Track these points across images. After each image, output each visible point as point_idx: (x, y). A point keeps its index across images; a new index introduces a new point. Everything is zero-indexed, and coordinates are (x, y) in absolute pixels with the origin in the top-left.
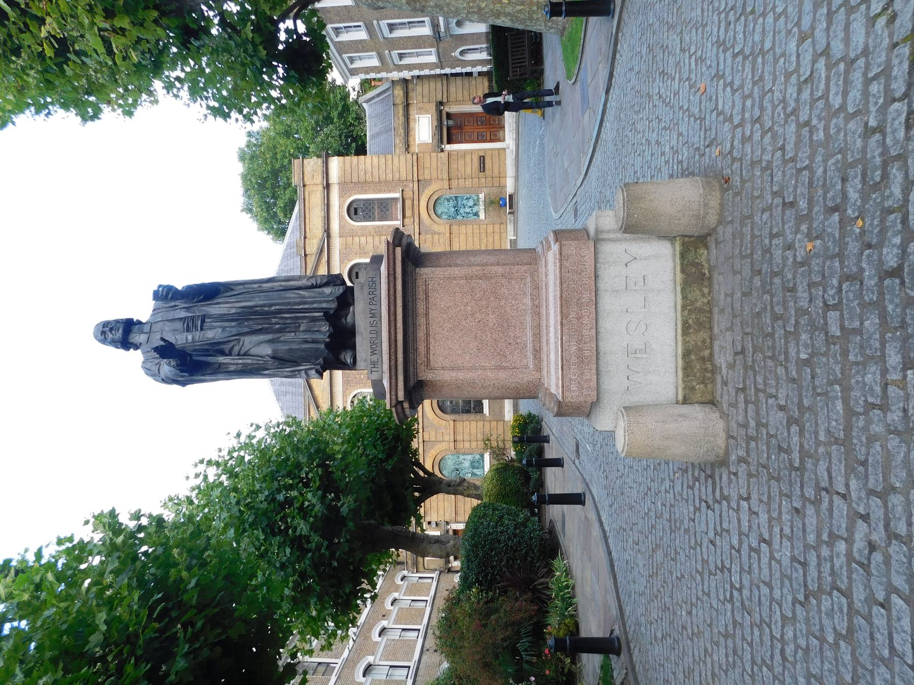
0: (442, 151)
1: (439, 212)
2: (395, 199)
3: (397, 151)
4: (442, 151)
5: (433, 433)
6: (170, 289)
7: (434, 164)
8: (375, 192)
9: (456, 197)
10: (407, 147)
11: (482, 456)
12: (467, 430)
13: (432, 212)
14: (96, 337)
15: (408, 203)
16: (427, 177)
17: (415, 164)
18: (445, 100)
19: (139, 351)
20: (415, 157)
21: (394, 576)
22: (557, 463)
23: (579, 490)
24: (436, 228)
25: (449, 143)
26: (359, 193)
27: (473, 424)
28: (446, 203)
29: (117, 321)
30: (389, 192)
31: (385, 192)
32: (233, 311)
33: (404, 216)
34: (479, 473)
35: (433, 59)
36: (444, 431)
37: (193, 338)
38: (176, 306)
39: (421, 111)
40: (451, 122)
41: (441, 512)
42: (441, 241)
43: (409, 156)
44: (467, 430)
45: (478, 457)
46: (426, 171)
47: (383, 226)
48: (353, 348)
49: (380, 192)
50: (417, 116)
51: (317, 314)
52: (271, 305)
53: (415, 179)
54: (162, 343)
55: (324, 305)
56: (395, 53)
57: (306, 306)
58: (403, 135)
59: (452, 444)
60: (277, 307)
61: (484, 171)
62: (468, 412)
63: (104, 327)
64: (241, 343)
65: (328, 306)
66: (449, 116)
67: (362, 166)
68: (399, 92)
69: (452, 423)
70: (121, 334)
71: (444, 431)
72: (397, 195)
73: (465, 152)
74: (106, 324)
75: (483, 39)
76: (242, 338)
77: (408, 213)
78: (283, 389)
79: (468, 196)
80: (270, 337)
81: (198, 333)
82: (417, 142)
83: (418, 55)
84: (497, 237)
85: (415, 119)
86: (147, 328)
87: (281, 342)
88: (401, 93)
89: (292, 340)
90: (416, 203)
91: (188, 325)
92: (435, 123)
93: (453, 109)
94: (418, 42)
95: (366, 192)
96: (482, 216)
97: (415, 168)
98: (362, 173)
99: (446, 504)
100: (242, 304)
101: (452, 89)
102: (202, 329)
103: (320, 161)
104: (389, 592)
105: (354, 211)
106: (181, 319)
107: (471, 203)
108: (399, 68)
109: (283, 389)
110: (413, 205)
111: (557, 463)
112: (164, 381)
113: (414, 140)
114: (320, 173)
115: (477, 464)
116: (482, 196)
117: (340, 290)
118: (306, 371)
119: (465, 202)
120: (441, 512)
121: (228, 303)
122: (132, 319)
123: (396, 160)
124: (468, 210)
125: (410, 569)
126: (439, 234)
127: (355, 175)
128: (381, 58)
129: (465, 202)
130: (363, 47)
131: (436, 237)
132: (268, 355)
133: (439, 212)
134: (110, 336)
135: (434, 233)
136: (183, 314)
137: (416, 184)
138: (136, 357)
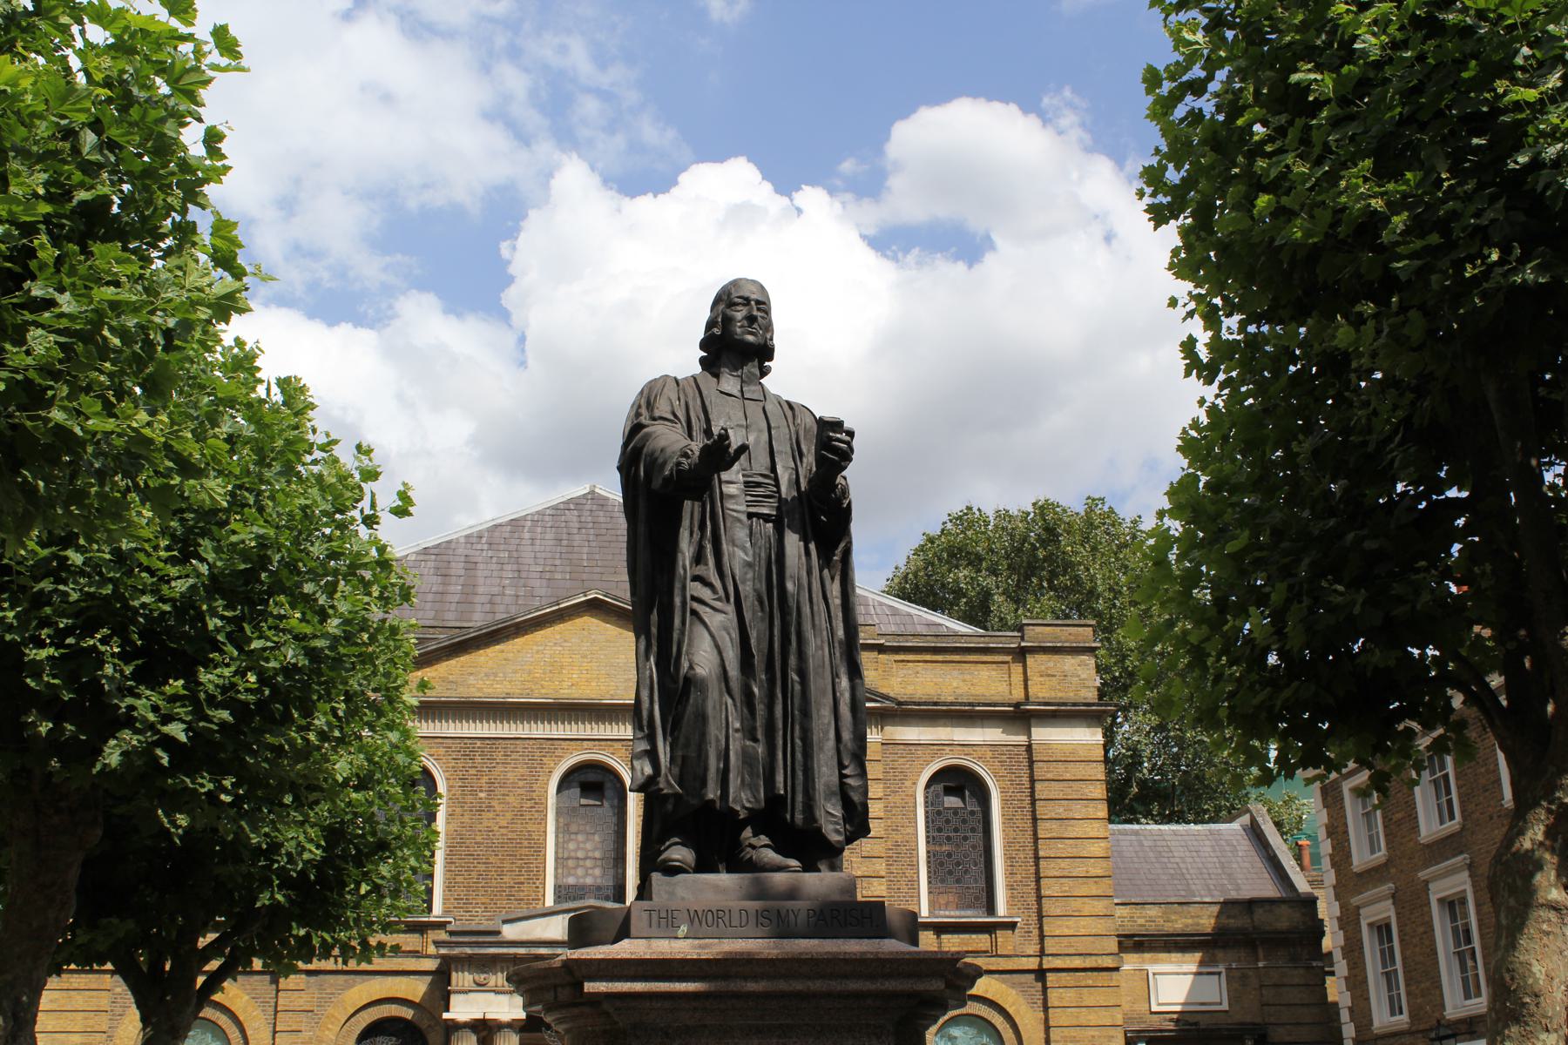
1: (956, 1032)
2: (991, 908)
3: (1121, 911)
5: (301, 1001)
6: (846, 456)
7: (1092, 1018)
8: (1008, 845)
10: (1135, 943)
14: (735, 283)
17: (1089, 962)
19: (698, 369)
20: (1108, 962)
26: (1005, 802)
29: (768, 327)
30: (1010, 887)
31: (1010, 873)
32: (790, 586)
35: (1382, 1019)
36: (306, 1035)
37: (732, 497)
38: (801, 455)
39: (1237, 982)
43: (1113, 945)
47: (915, 866)
48: (703, 866)
49: (1010, 859)
50: (1221, 968)
51: (780, 778)
52: (803, 673)
53: (1048, 963)
54: (734, 446)
55: (800, 798)
56: (1385, 910)
57: (799, 756)
58: (1168, 928)
60: (797, 687)
63: (758, 302)
64: (718, 604)
65: (799, 806)
67: (1078, 810)
70: (737, 336)
71: (306, 1035)
74: (763, 305)
76: (731, 608)
80: (734, 671)
81: (743, 508)
82: (1152, 968)
83: (1390, 977)
86: (751, 391)
87: (721, 695)
88: (1283, 925)
89: (724, 720)
91: (759, 485)
92: (1204, 1022)
94: (1423, 976)
95: (1008, 820)
97: (1077, 962)
98: (1059, 810)
100: (806, 610)
102: (750, 516)
103: (1091, 695)
105: (957, 781)
106: (773, 469)
108: (1349, 921)
109: (458, 568)
112: (635, 429)
113: (1156, 962)
114: (1060, 695)
117: (832, 831)
118: (652, 755)
121: (809, 573)
122: (771, 358)
123: (1099, 906)
127: (1054, 790)
128: (1374, 875)
130: (1399, 823)
132: (691, 667)
134: (739, 316)
136: (784, 477)
137: (1033, 963)
138: (686, 360)
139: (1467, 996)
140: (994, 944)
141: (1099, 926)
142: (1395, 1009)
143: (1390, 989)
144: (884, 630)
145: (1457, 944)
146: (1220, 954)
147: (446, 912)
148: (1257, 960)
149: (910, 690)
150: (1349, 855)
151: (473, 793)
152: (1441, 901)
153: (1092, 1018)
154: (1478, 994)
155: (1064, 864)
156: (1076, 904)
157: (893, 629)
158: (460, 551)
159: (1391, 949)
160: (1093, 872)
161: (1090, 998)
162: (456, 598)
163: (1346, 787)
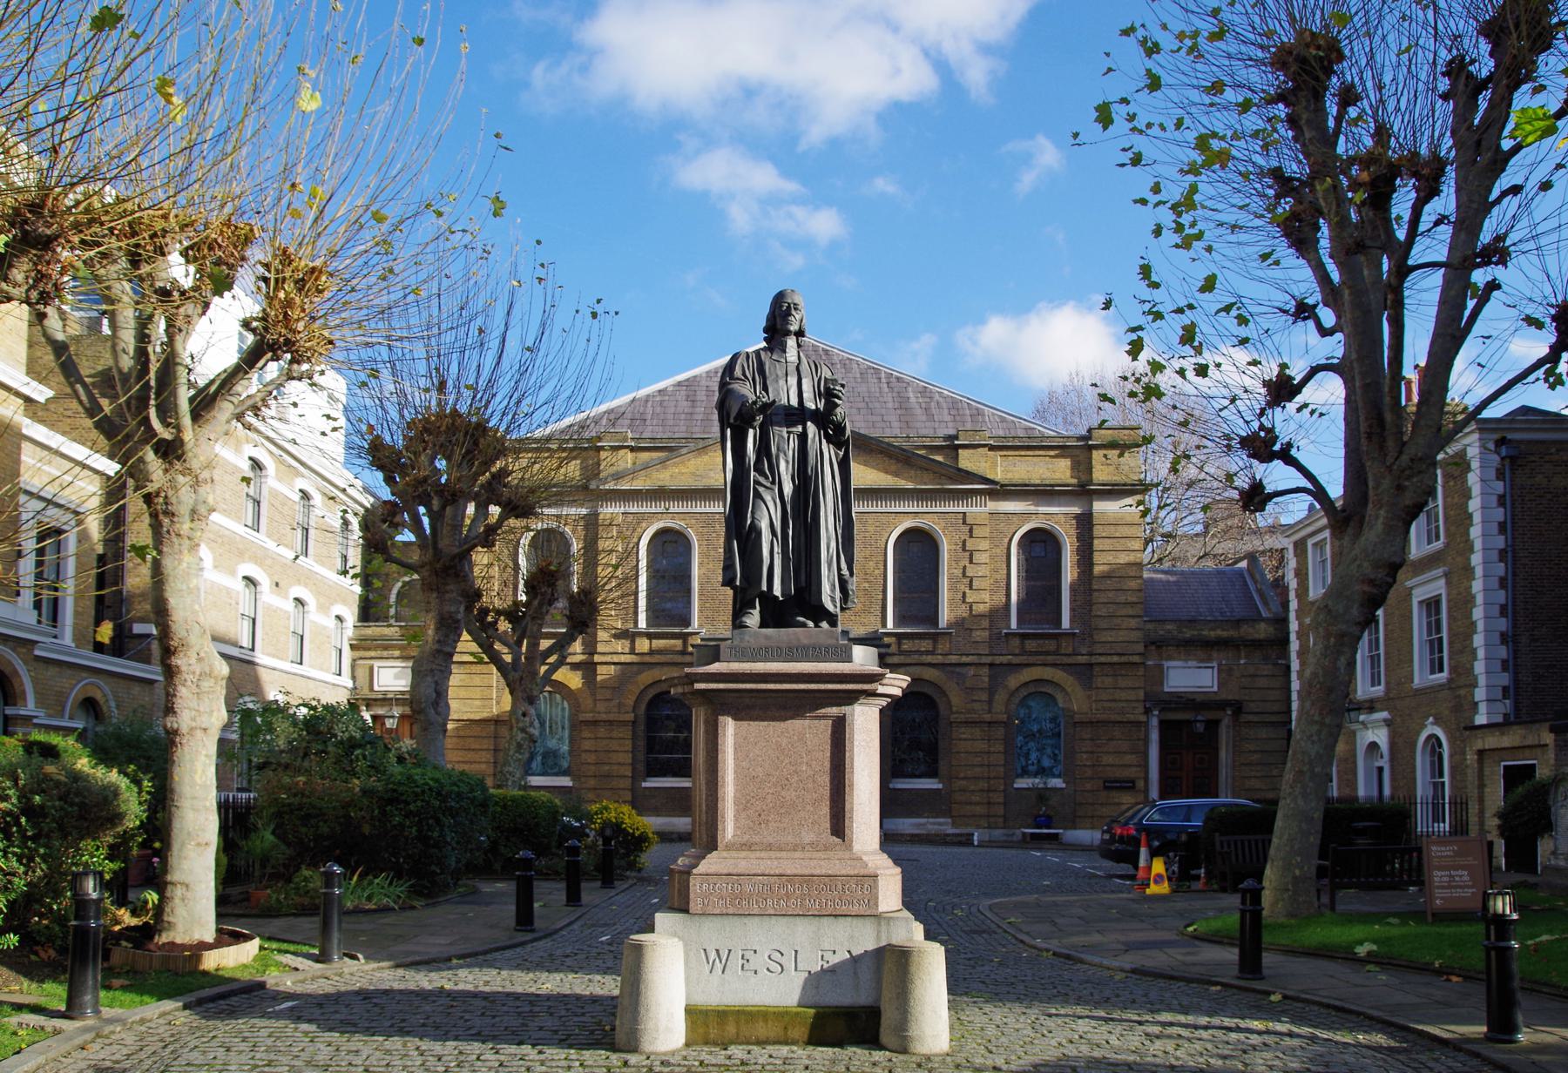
0: (1147, 711)
3: (1149, 626)
4: (1147, 711)
7: (1124, 695)
9: (1059, 735)
11: (564, 773)
12: (614, 745)
13: (1032, 689)
15: (1051, 645)
16: (1098, 682)
17: (1124, 659)
18: (1244, 718)
20: (1136, 659)
21: (344, 602)
22: (573, 898)
23: (537, 923)
24: (1001, 697)
25: (1162, 723)
27: (628, 758)
28: (1049, 715)
30: (1072, 610)
33: (1024, 636)
34: (534, 765)
39: (1225, 674)
40: (1200, 727)
41: (463, 693)
42: (977, 706)
43: (1140, 648)
44: (614, 745)
45: (565, 765)
46: (1108, 681)
50: (1215, 664)
53: (1094, 660)
59: (589, 716)
61: (1106, 788)
62: (650, 749)
66: (1213, 725)
68: (1263, 631)
69: (630, 717)
72: (1066, 623)
73: (1145, 755)
75: (1347, 791)
77: (1031, 645)
78: (701, 395)
79: (1061, 757)
82: (1166, 664)
84: (978, 810)
85: (1210, 660)
90: (1050, 659)
92: (1199, 698)
93: (1224, 735)
96: (1022, 783)
97: (1116, 659)
99: (478, 703)
101: (1263, 733)
104: (318, 594)
107: (1046, 763)
110: (1047, 653)
111: (573, 898)
113: (1170, 658)
114: (1117, 479)
115: (550, 762)
116: (1057, 783)
119: (1049, 751)
120: (463, 693)
123: (1133, 623)
124: (1033, 756)
125: (358, 632)
126: (990, 702)
129: (1049, 751)
131: (985, 697)
133: (1032, 704)
135: (992, 691)
139: (1432, 672)
140: (1059, 646)
141: (1135, 635)
142: (1375, 681)
143: (1372, 667)
144: (995, 433)
145: (1430, 634)
146: (1215, 655)
147: (701, 626)
148: (1239, 658)
149: (1010, 476)
150: (1307, 590)
151: (715, 549)
152: (1420, 603)
153: (1124, 695)
154: (1441, 670)
155: (1111, 595)
156: (1119, 621)
157: (1001, 433)
158: (704, 383)
159: (1377, 639)
160: (1130, 599)
161: (1122, 682)
162: (700, 417)
163: (1310, 542)
